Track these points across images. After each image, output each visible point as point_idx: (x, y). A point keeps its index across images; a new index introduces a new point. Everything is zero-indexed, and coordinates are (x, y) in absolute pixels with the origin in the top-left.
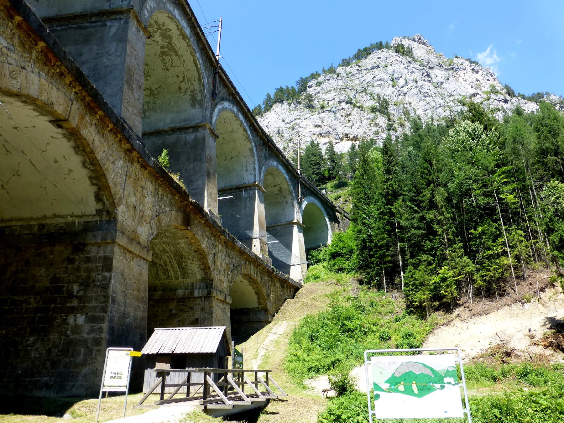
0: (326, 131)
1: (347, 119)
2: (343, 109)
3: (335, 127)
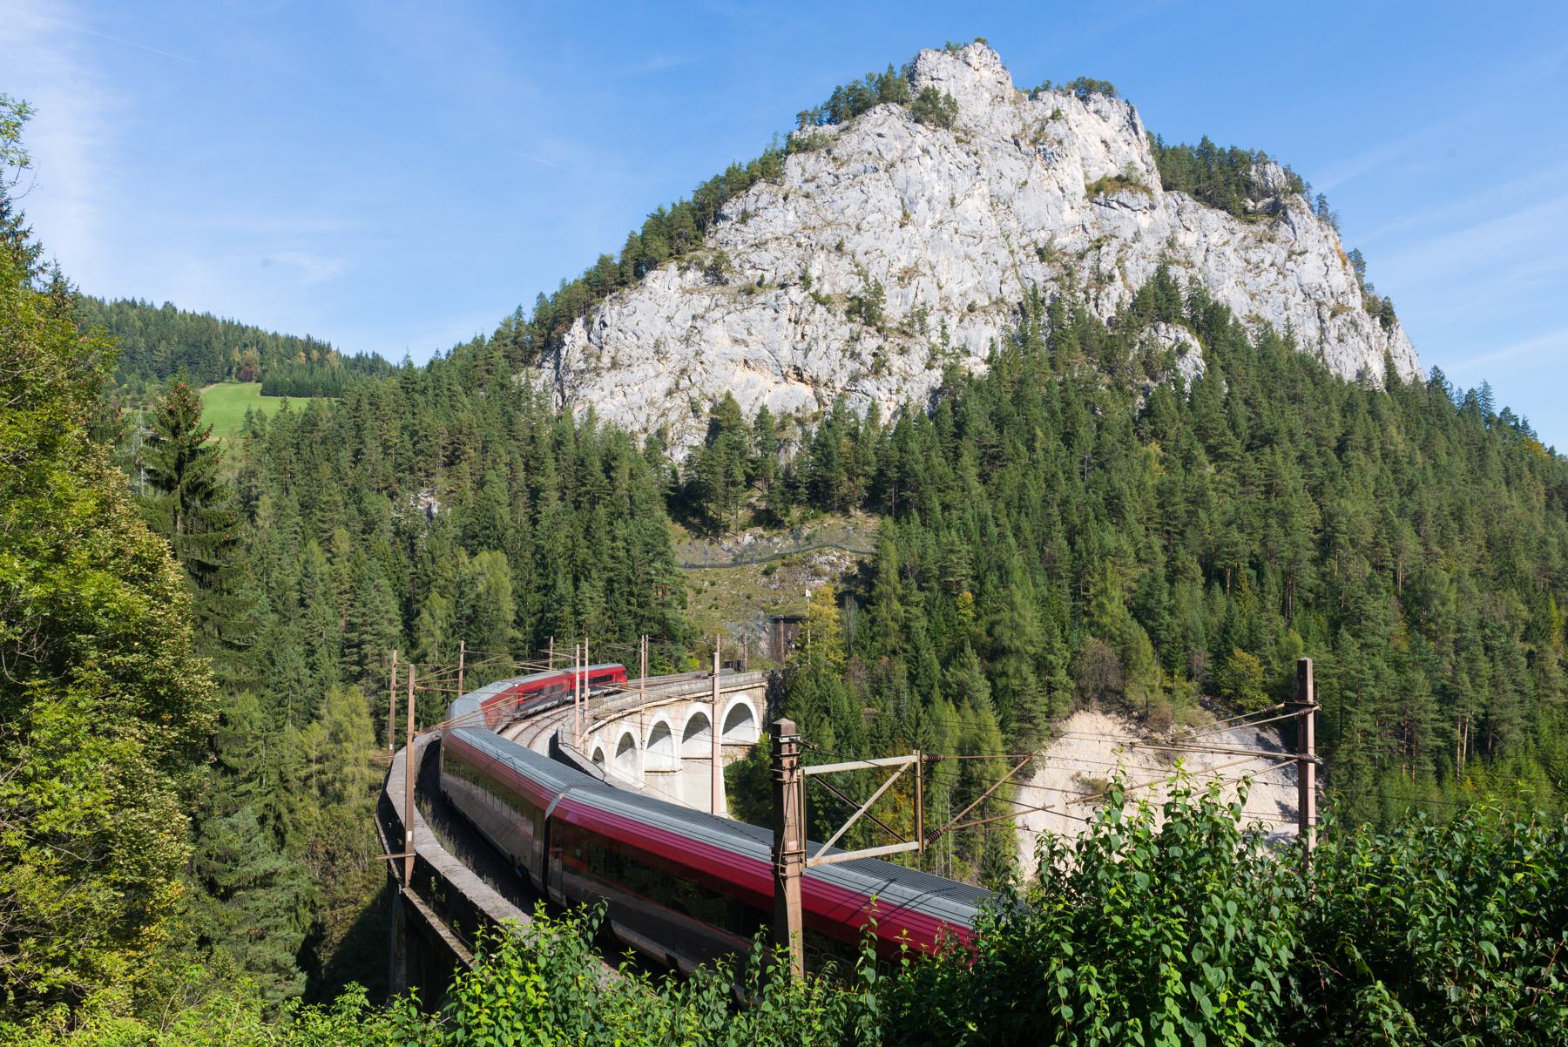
2: (792, 303)
3: (776, 346)
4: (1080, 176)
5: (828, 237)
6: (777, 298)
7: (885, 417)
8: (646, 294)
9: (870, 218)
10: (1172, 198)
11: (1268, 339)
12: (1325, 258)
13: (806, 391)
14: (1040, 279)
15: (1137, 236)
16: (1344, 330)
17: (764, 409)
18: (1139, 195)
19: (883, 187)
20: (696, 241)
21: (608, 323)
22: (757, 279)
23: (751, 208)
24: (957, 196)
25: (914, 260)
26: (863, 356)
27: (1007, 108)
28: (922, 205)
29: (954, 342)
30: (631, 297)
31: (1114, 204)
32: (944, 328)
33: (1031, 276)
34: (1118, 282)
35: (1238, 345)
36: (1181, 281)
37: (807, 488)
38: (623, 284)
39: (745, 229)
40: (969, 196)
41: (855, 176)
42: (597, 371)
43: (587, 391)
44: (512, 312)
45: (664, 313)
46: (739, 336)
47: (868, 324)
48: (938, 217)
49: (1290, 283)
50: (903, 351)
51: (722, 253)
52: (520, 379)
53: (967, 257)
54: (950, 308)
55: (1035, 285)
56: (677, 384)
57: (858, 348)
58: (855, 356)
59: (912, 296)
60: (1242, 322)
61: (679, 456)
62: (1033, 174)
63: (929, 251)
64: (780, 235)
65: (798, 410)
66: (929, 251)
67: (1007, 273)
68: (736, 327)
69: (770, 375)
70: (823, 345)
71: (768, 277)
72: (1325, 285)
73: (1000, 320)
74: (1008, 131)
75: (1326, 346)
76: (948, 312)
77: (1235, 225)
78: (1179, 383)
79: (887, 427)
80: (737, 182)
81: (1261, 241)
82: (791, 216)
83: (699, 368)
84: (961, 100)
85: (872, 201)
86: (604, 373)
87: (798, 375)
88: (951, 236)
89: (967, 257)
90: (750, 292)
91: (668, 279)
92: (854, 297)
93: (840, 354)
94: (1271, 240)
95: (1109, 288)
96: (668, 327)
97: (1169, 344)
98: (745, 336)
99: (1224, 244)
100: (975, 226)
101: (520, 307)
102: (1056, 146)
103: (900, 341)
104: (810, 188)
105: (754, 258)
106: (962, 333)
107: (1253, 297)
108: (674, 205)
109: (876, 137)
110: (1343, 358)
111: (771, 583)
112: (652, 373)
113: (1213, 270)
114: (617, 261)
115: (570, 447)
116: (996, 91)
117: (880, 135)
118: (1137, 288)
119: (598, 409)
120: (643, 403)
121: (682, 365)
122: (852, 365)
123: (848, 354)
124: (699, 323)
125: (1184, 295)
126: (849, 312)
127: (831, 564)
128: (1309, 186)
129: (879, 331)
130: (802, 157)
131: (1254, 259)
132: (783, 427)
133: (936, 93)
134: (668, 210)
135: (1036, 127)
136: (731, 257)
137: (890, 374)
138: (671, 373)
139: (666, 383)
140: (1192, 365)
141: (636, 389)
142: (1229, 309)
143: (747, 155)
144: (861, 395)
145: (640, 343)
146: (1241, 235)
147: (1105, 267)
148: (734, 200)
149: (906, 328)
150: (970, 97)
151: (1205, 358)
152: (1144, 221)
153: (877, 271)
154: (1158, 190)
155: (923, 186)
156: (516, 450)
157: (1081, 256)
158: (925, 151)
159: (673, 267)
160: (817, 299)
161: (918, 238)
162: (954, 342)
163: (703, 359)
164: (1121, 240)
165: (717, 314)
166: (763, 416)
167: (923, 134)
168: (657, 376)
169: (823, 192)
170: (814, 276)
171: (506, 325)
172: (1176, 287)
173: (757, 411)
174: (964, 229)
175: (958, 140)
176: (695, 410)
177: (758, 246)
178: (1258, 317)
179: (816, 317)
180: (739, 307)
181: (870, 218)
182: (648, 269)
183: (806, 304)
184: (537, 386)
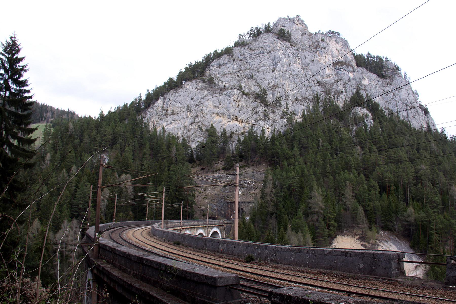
1: (237, 103)
3: (229, 109)
4: (331, 59)
5: (247, 73)
6: (230, 93)
7: (268, 134)
8: (185, 90)
9: (262, 68)
10: (360, 69)
11: (391, 113)
12: (407, 91)
13: (241, 125)
14: (319, 91)
15: (349, 80)
16: (415, 114)
17: (224, 129)
18: (349, 67)
19: (266, 58)
20: (202, 73)
21: (171, 99)
22: (223, 87)
23: (222, 64)
24: (291, 63)
25: (277, 83)
26: (259, 113)
27: (307, 37)
28: (279, 65)
29: (290, 110)
30: (179, 91)
31: (342, 70)
32: (287, 105)
33: (315, 90)
34: (344, 94)
35: (383, 116)
36: (364, 95)
37: (239, 157)
38: (177, 86)
39: (220, 70)
40: (295, 63)
41: (257, 55)
42: (166, 115)
43: (162, 122)
44: (138, 95)
45: (190, 96)
47: (262, 102)
48: (285, 69)
49: (397, 98)
50: (273, 112)
51: (211, 77)
52: (138, 118)
53: (294, 83)
54: (289, 99)
55: (317, 93)
56: (194, 121)
57: (258, 110)
58: (257, 113)
59: (276, 94)
60: (383, 109)
61: (194, 145)
62: (316, 58)
63: (282, 80)
64: (231, 72)
65: (236, 131)
66: (282, 80)
67: (308, 89)
68: (215, 102)
69: (226, 119)
70: (245, 109)
71: (227, 85)
72: (408, 99)
73: (305, 104)
74: (307, 43)
75: (409, 118)
76: (288, 100)
77: (379, 79)
78: (366, 127)
79: (267, 137)
80: (217, 55)
81: (388, 84)
82: (235, 66)
83: (202, 116)
84: (292, 33)
85: (263, 62)
86: (169, 116)
87: (236, 119)
88: (289, 75)
89: (294, 83)
90: (221, 90)
91: (192, 85)
92: (256, 94)
93: (251, 112)
94: (391, 85)
95: (342, 95)
96: (192, 101)
97: (361, 114)
98: (218, 105)
99: (377, 84)
100: (297, 73)
101: (141, 94)
102: (323, 49)
103: (272, 109)
104: (241, 57)
106: (293, 108)
107: (386, 102)
108: (195, 61)
109: (264, 43)
110: (414, 123)
111: (226, 190)
112: (185, 116)
113: (373, 92)
114: (175, 79)
115: (155, 140)
116: (303, 32)
117: (265, 42)
118: (350, 97)
119: (166, 128)
120: (182, 127)
121: (196, 114)
122: (255, 116)
123: (254, 112)
124: (202, 100)
125: (365, 100)
126: (255, 98)
127: (248, 184)
128: (401, 69)
129: (265, 105)
130: (239, 48)
131: (386, 90)
132: (231, 136)
133: (284, 31)
134: (193, 64)
135: (317, 43)
136: (214, 79)
137: (269, 120)
138: (192, 117)
139: (190, 120)
140: (369, 122)
141: (179, 122)
142: (379, 104)
143: (221, 48)
144: (258, 127)
145: (182, 106)
146: (381, 82)
147: (340, 88)
148: (216, 60)
149: (274, 105)
150: (295, 33)
151: (373, 119)
152: (351, 75)
153: (264, 85)
154: (356, 67)
155: (280, 59)
156: (136, 141)
157: (333, 84)
158: (280, 48)
159: (194, 81)
160: (244, 93)
161: (278, 76)
162: (290, 110)
163: (203, 112)
164: (344, 81)
166: (224, 133)
167: (279, 43)
168: (187, 118)
169: (246, 59)
170: (243, 86)
171: (136, 99)
172: (363, 97)
173: (222, 131)
174: (293, 73)
175: (291, 45)
176: (202, 130)
177: (224, 75)
178: (388, 108)
179: (243, 99)
180: (216, 95)
181: (262, 68)
182: (186, 82)
184: (145, 120)
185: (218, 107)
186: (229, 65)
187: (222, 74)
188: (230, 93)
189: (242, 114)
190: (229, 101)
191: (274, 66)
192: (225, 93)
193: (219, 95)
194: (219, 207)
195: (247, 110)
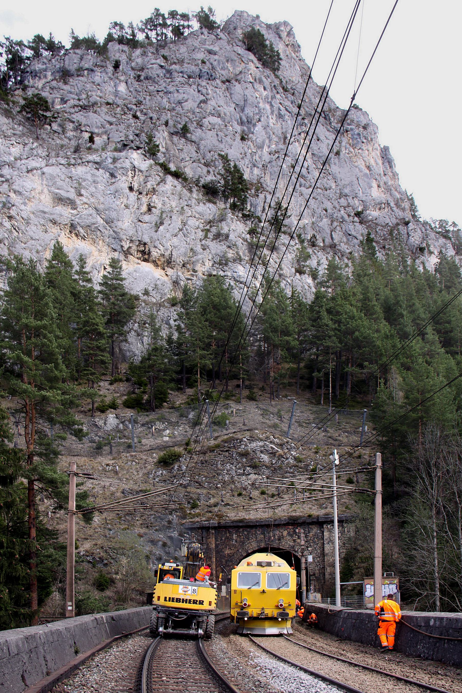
0: (88, 222)
1: (144, 200)
3: (113, 215)
23: (72, 68)
39: (67, 87)
46: (63, 193)
64: (111, 101)
68: (60, 183)
70: (177, 222)
87: (143, 252)
93: (200, 234)
105: (79, 117)
123: (210, 235)
165: (33, 164)
183: (153, 173)
185: (72, 204)
186: (98, 77)
187: (76, 103)
188: (115, 160)
189: (168, 235)
190: (112, 188)
191: (245, 128)
192: (98, 159)
193: (73, 161)
194: (164, 545)
195: (184, 224)
